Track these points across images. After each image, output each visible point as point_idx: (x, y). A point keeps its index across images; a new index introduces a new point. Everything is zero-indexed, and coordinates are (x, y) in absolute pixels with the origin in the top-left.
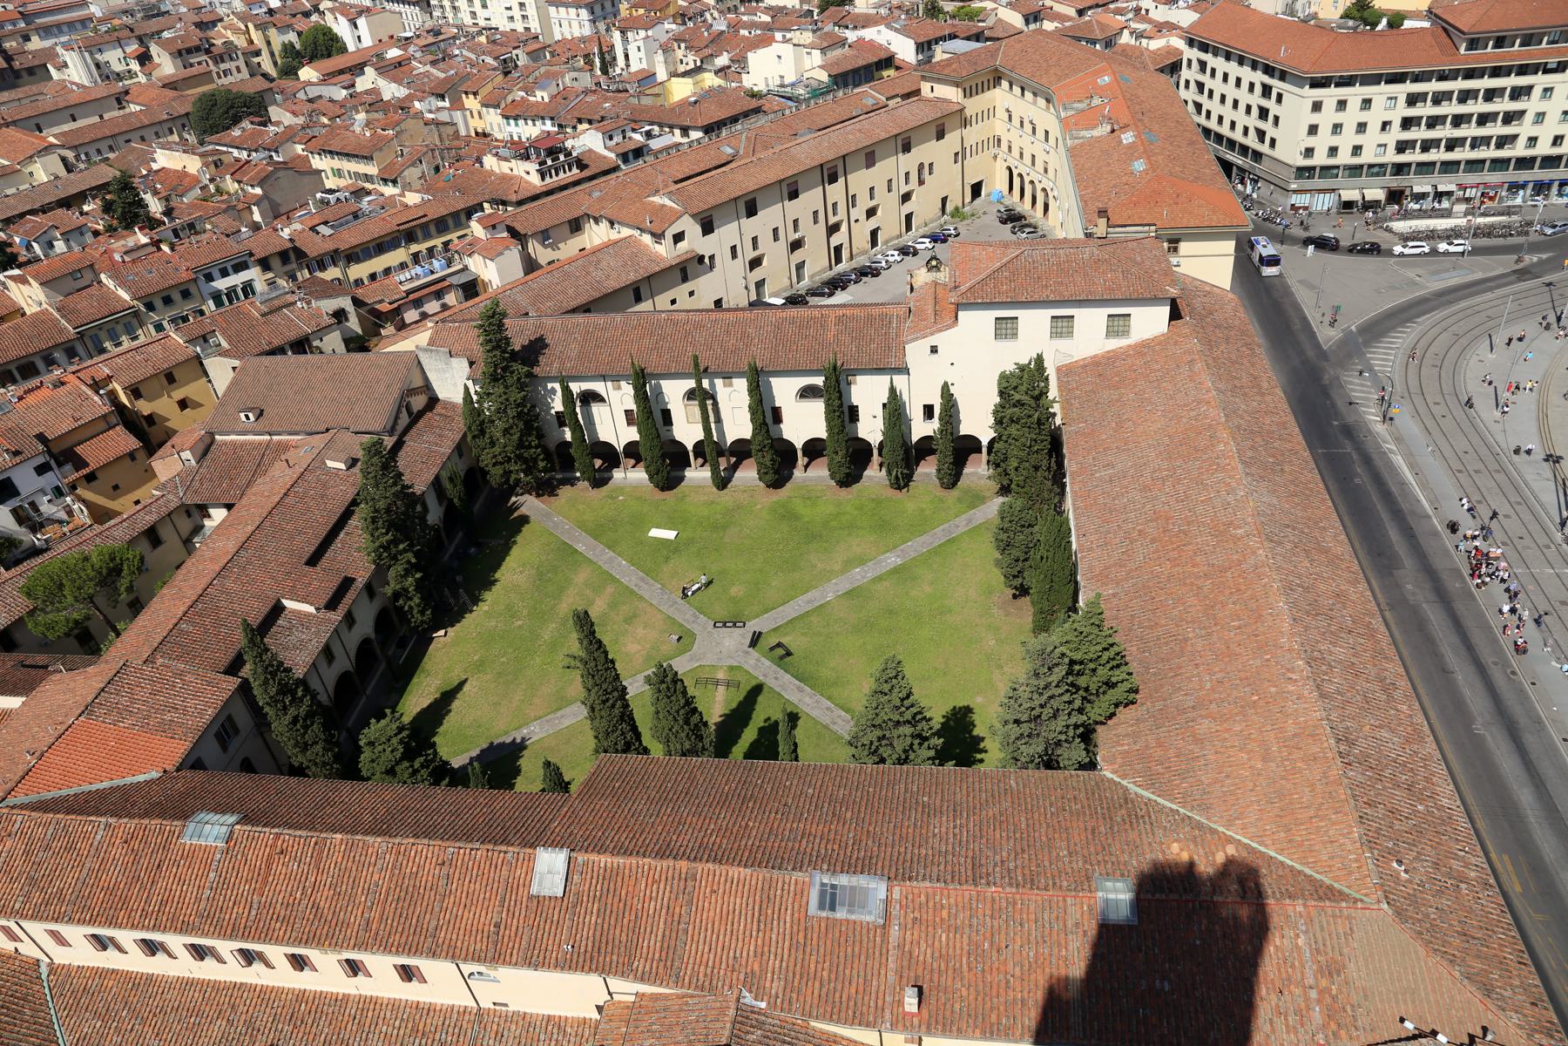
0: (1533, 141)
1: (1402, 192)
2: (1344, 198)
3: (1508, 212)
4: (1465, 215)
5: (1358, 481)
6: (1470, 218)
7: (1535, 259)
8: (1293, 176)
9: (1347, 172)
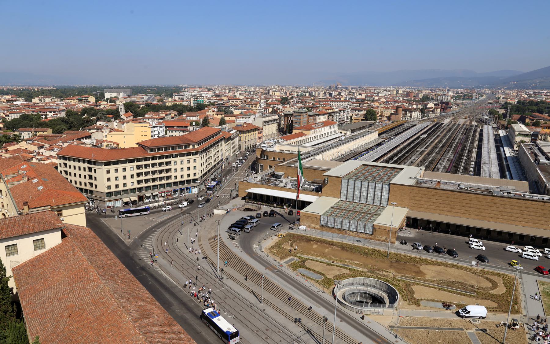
0: (176, 177)
1: (142, 197)
2: (124, 201)
3: (175, 198)
4: (163, 201)
5: (150, 283)
6: (165, 202)
7: (186, 209)
8: (105, 196)
9: (123, 192)
